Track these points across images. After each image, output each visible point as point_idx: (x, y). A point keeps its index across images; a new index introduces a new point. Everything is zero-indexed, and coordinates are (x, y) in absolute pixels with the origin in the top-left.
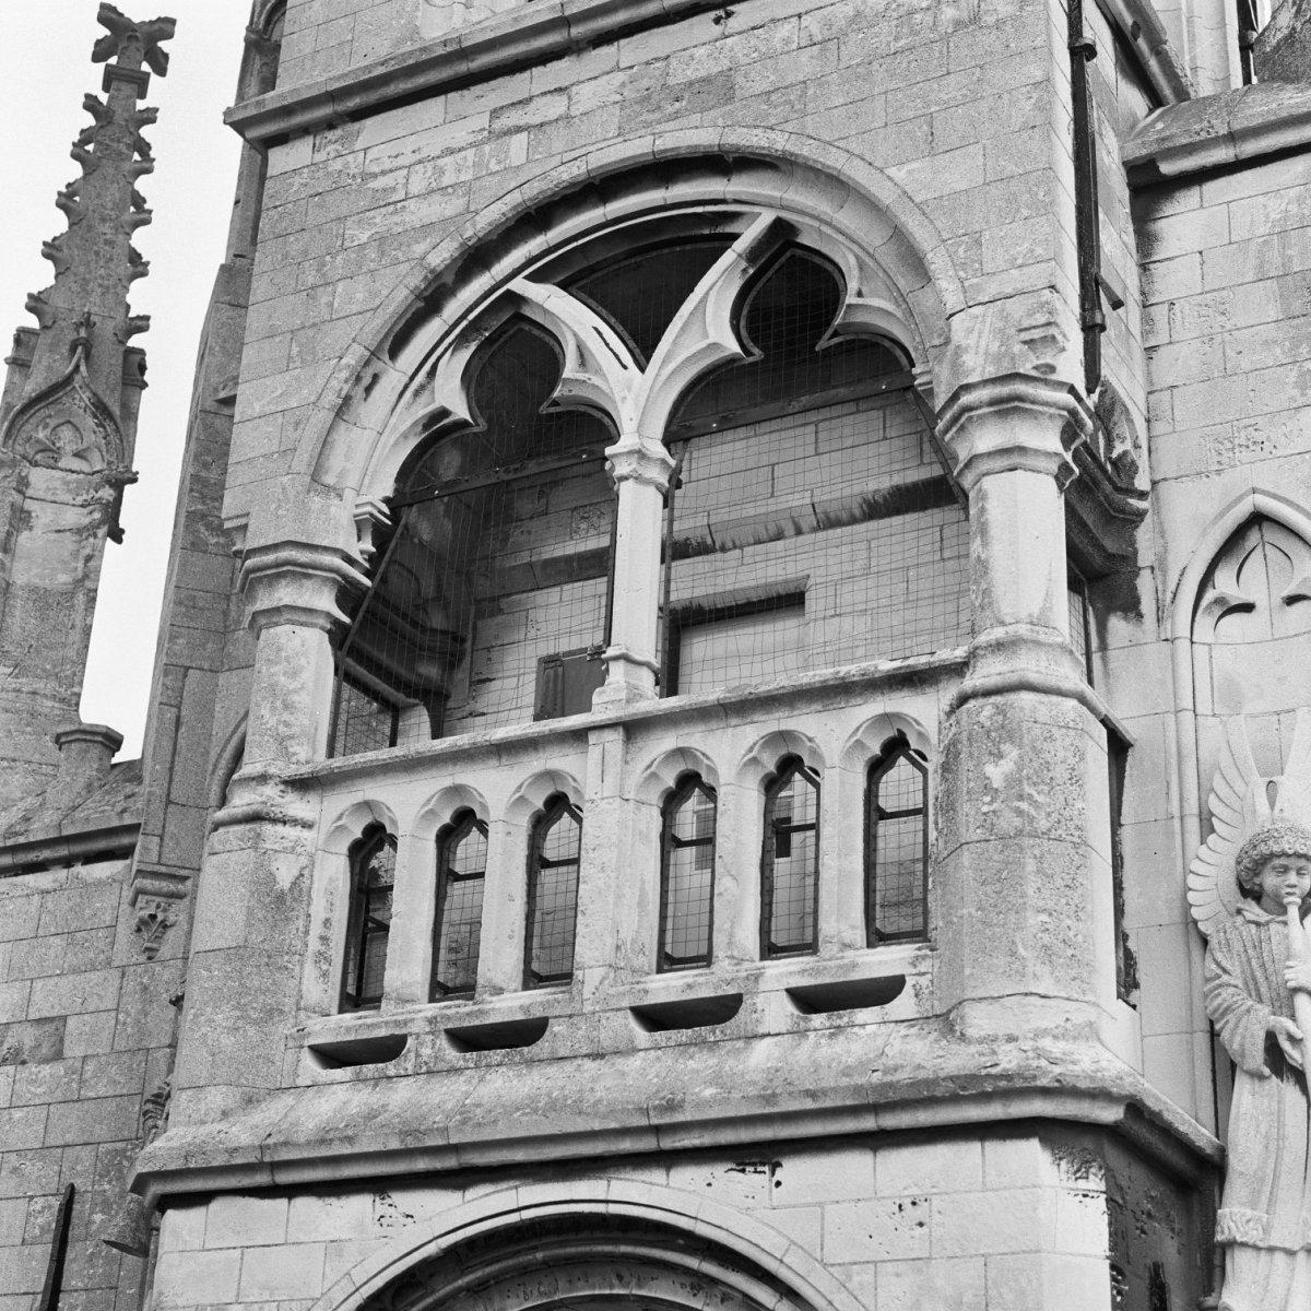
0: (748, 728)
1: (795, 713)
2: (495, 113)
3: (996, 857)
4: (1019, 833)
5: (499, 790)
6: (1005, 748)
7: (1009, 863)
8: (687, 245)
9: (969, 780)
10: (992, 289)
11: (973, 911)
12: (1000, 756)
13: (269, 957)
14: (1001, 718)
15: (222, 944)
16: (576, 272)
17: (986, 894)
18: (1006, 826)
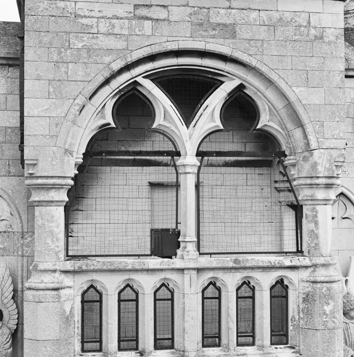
0: (238, 274)
1: (253, 271)
2: (136, 6)
3: (327, 335)
4: (334, 328)
5: (147, 284)
6: (330, 301)
7: (331, 337)
8: (206, 83)
9: (319, 310)
10: (327, 144)
11: (321, 350)
12: (328, 304)
13: (66, 341)
14: (328, 291)
15: (50, 338)
16: (162, 80)
17: (324, 346)
18: (330, 326)
